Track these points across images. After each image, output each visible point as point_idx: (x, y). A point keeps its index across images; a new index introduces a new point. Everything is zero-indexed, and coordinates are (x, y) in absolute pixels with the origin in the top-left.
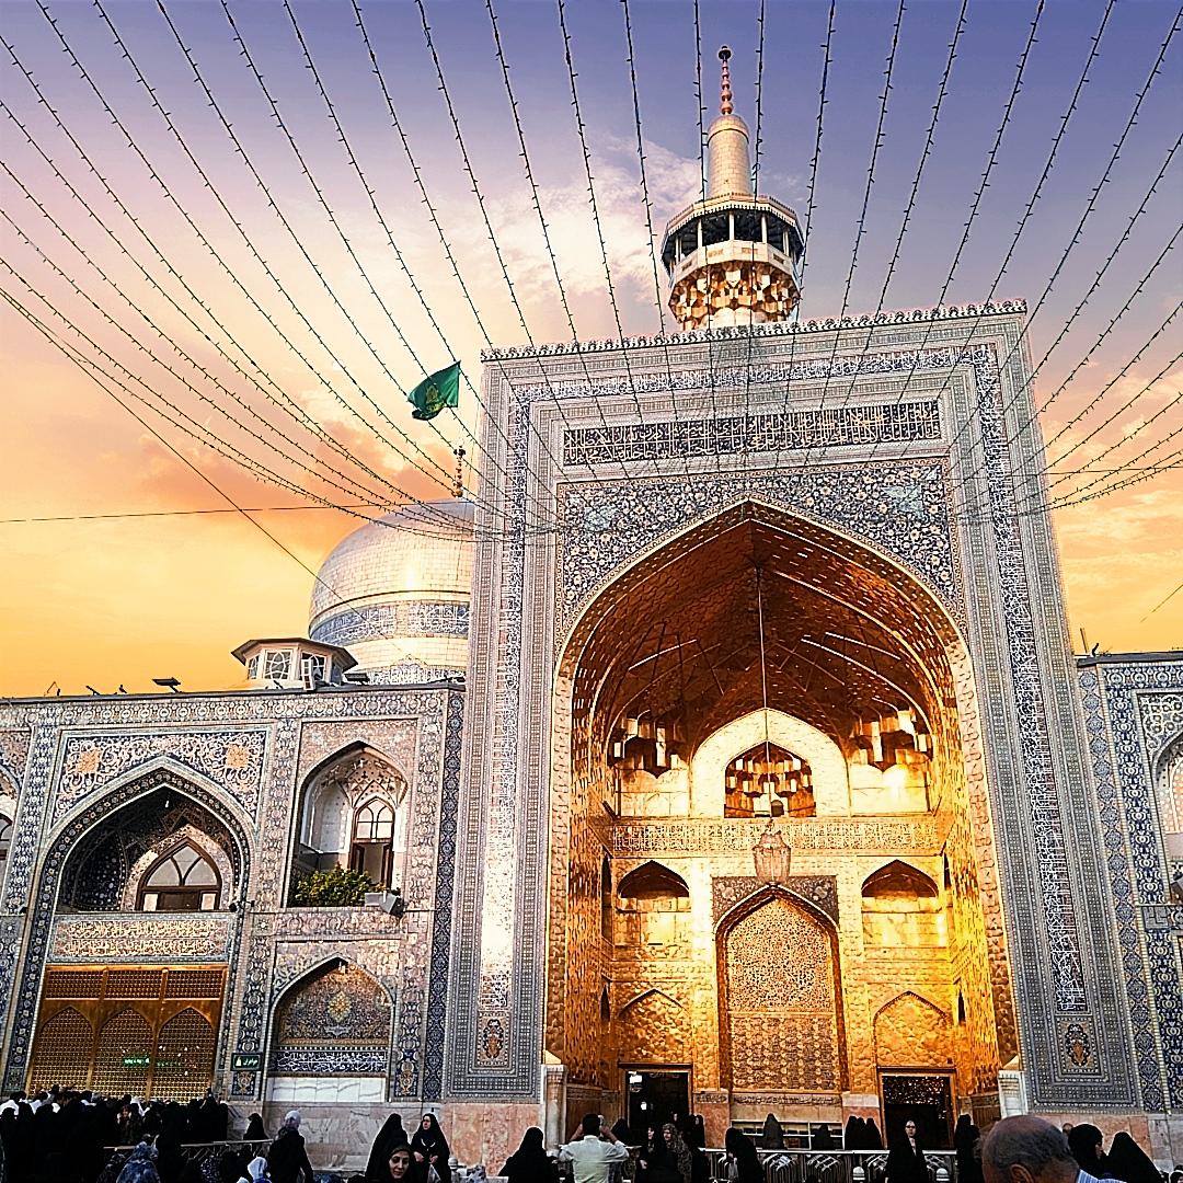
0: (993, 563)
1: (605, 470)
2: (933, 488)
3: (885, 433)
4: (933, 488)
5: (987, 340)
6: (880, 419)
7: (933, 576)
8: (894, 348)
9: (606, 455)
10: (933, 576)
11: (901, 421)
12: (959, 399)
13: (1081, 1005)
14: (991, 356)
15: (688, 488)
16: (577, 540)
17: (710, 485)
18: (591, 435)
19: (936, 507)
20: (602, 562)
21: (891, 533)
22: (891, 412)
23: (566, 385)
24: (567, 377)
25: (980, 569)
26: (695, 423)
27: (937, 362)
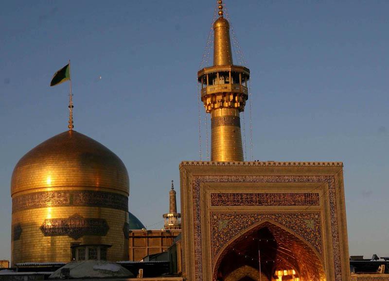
0: (331, 245)
1: (222, 208)
2: (317, 221)
3: (305, 203)
4: (317, 221)
5: (332, 175)
6: (304, 197)
7: (316, 248)
8: (307, 174)
9: (224, 203)
10: (316, 248)
11: (311, 200)
12: (324, 193)
14: (333, 179)
15: (249, 216)
16: (217, 231)
17: (256, 215)
18: (219, 196)
19: (317, 227)
20: (225, 239)
21: (306, 234)
22: (307, 195)
23: (211, 177)
24: (210, 174)
25: (328, 247)
26: (251, 194)
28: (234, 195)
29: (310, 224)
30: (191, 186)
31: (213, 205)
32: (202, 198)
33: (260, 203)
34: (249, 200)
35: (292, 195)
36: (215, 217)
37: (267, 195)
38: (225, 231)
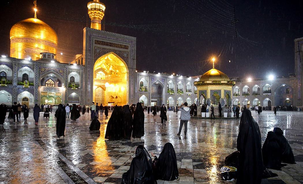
1: (99, 46)
6: (124, 46)
9: (99, 44)
11: (126, 47)
12: (130, 46)
13: (133, 98)
18: (98, 41)
27: (129, 42)
28: (102, 42)
29: (125, 55)
30: (88, 36)
31: (95, 44)
32: (92, 41)
33: (110, 46)
34: (107, 44)
35: (121, 45)
36: (96, 48)
37: (113, 43)
38: (99, 53)
